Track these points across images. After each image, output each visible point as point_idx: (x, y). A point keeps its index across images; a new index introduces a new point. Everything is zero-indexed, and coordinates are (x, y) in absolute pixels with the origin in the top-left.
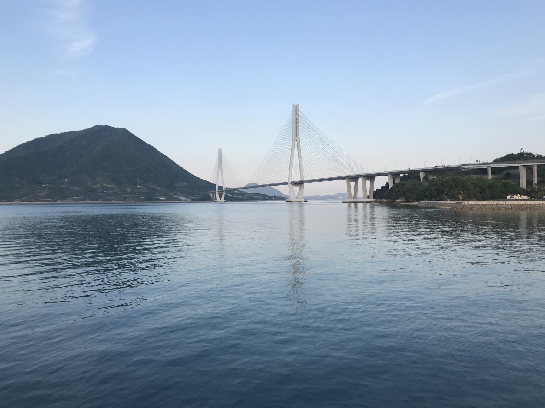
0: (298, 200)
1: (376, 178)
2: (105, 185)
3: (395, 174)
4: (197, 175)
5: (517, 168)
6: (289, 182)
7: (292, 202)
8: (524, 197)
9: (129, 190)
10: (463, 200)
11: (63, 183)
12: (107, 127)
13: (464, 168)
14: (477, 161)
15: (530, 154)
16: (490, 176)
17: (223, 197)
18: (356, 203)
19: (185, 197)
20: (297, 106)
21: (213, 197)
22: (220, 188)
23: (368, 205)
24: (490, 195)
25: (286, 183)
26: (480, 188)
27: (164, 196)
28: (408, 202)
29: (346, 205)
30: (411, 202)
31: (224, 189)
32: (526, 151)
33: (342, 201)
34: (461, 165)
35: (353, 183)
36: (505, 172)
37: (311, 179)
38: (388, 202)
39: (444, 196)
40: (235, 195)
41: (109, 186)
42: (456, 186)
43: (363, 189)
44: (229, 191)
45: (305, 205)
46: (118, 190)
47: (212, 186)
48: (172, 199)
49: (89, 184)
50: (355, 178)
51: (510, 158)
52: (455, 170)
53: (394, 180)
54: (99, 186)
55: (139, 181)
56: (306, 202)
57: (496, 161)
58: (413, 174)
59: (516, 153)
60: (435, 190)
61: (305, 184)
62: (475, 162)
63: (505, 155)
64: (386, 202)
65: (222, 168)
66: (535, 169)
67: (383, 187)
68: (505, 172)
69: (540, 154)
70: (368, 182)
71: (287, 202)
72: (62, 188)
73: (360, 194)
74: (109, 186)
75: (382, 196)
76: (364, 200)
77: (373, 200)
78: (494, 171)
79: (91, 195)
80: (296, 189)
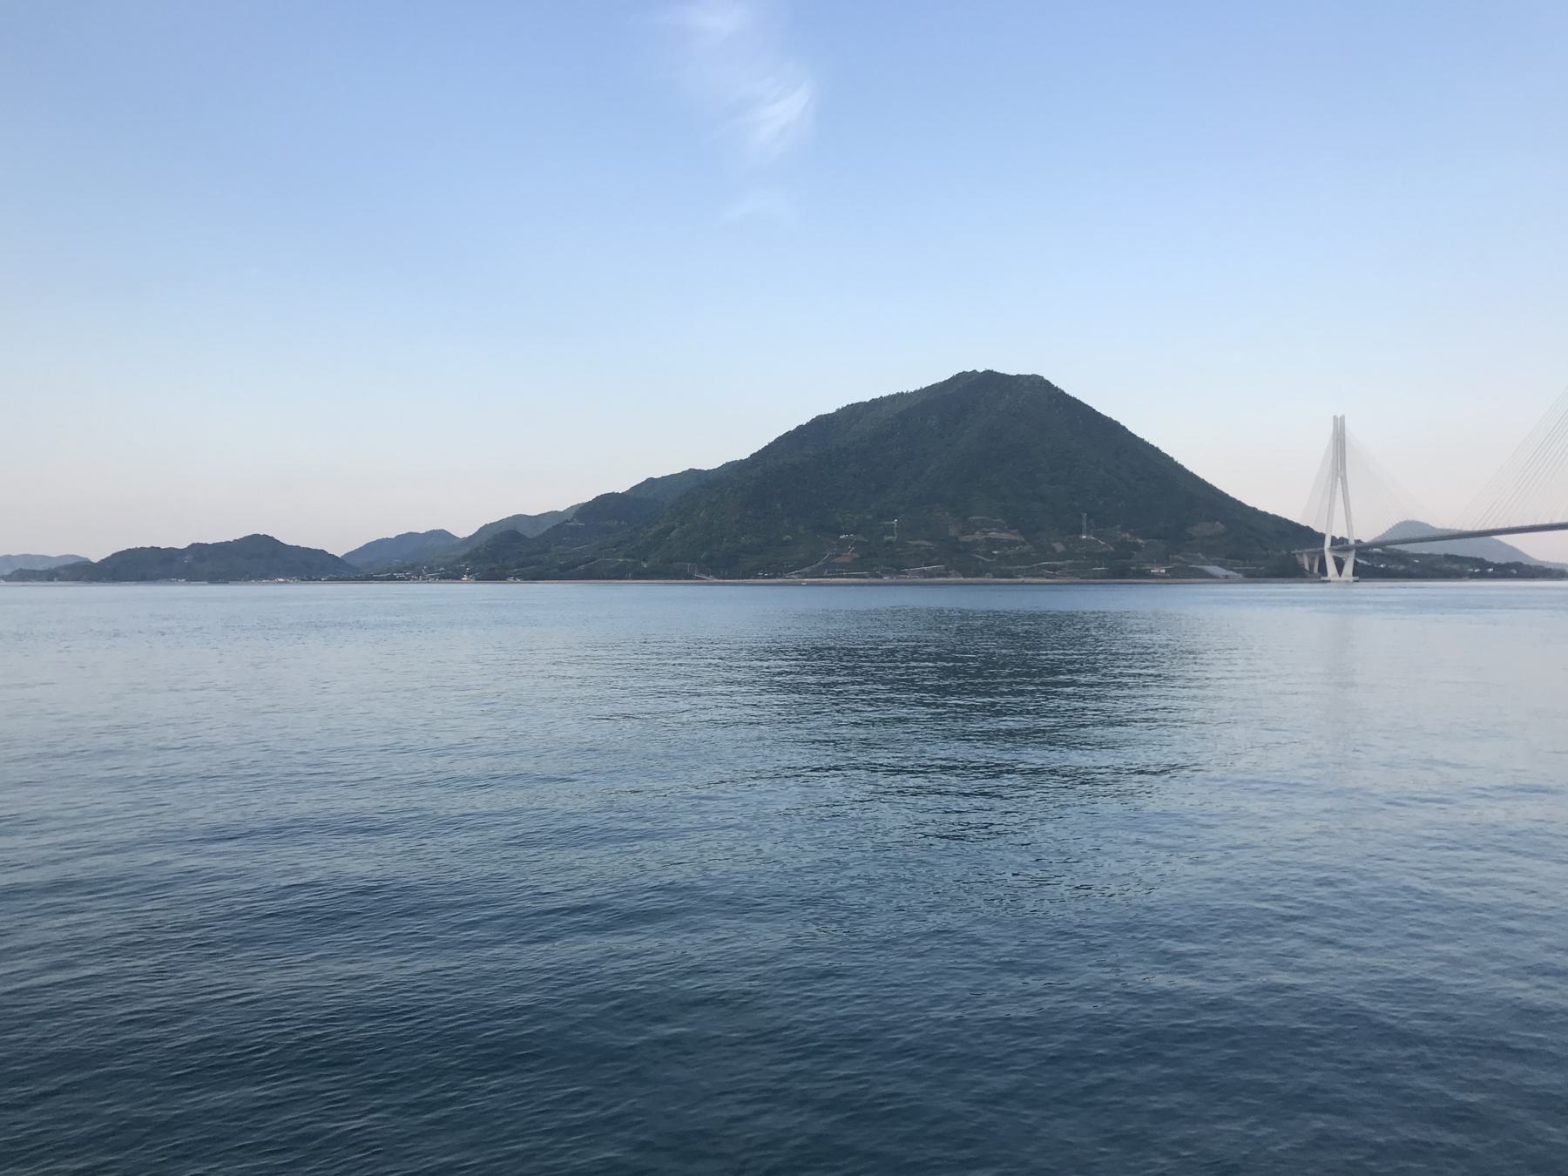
2: (993, 535)
4: (1249, 502)
9: (1060, 547)
11: (889, 530)
12: (990, 375)
17: (1348, 568)
19: (1221, 565)
21: (1311, 566)
27: (1164, 560)
31: (1352, 542)
41: (1005, 536)
44: (1362, 549)
46: (1028, 547)
47: (1309, 537)
48: (1183, 573)
49: (953, 532)
54: (978, 536)
55: (1084, 524)
72: (889, 543)
74: (1005, 536)
79: (964, 563)
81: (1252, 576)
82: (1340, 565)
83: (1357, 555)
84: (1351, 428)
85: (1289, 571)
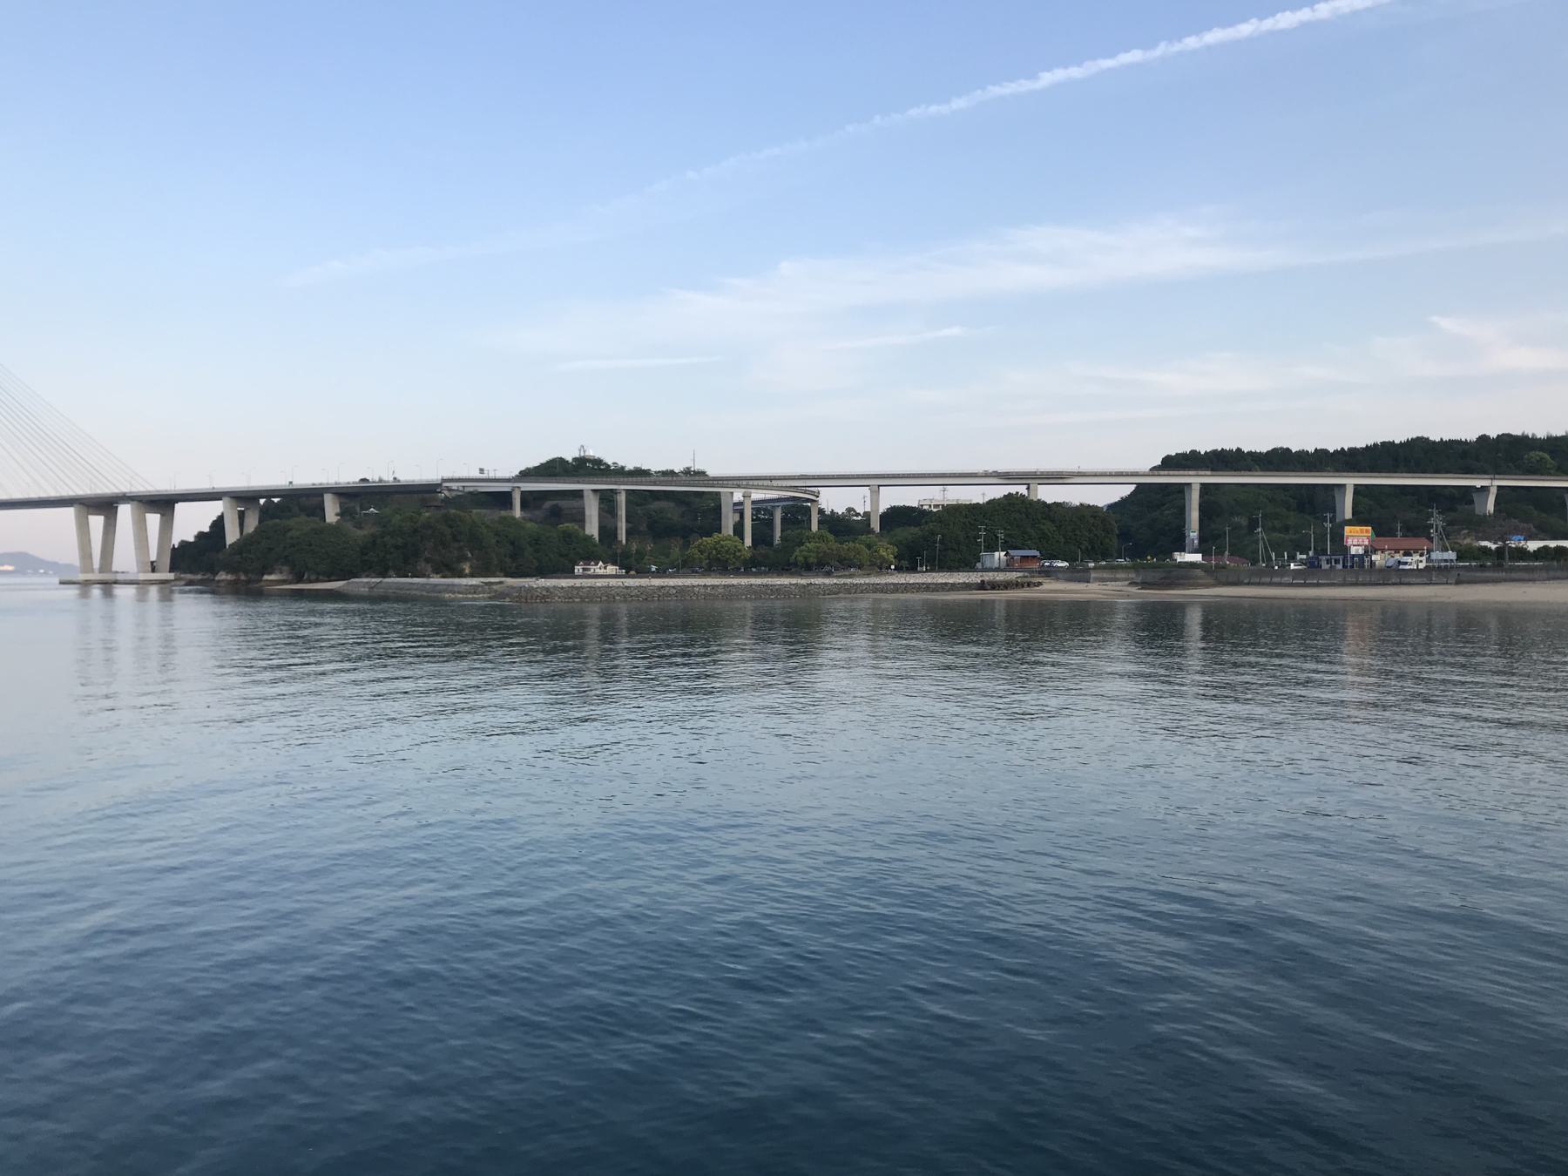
1: (179, 507)
3: (244, 499)
5: (579, 494)
8: (611, 569)
10: (472, 575)
13: (450, 490)
14: (482, 471)
15: (599, 462)
16: (517, 512)
18: (108, 586)
23: (154, 590)
24: (536, 563)
26: (512, 543)
28: (300, 580)
29: (73, 592)
30: (311, 582)
32: (591, 453)
33: (56, 580)
34: (444, 480)
35: (97, 522)
38: (236, 582)
39: (422, 565)
42: (455, 539)
43: (133, 543)
50: (106, 506)
51: (554, 468)
52: (424, 493)
53: (241, 516)
57: (526, 475)
58: (304, 501)
60: (397, 547)
63: (544, 460)
64: (230, 582)
66: (622, 499)
67: (201, 536)
68: (548, 504)
69: (621, 464)
70: (153, 520)
73: (126, 559)
75: (198, 563)
76: (142, 577)
77: (171, 576)
78: (529, 500)
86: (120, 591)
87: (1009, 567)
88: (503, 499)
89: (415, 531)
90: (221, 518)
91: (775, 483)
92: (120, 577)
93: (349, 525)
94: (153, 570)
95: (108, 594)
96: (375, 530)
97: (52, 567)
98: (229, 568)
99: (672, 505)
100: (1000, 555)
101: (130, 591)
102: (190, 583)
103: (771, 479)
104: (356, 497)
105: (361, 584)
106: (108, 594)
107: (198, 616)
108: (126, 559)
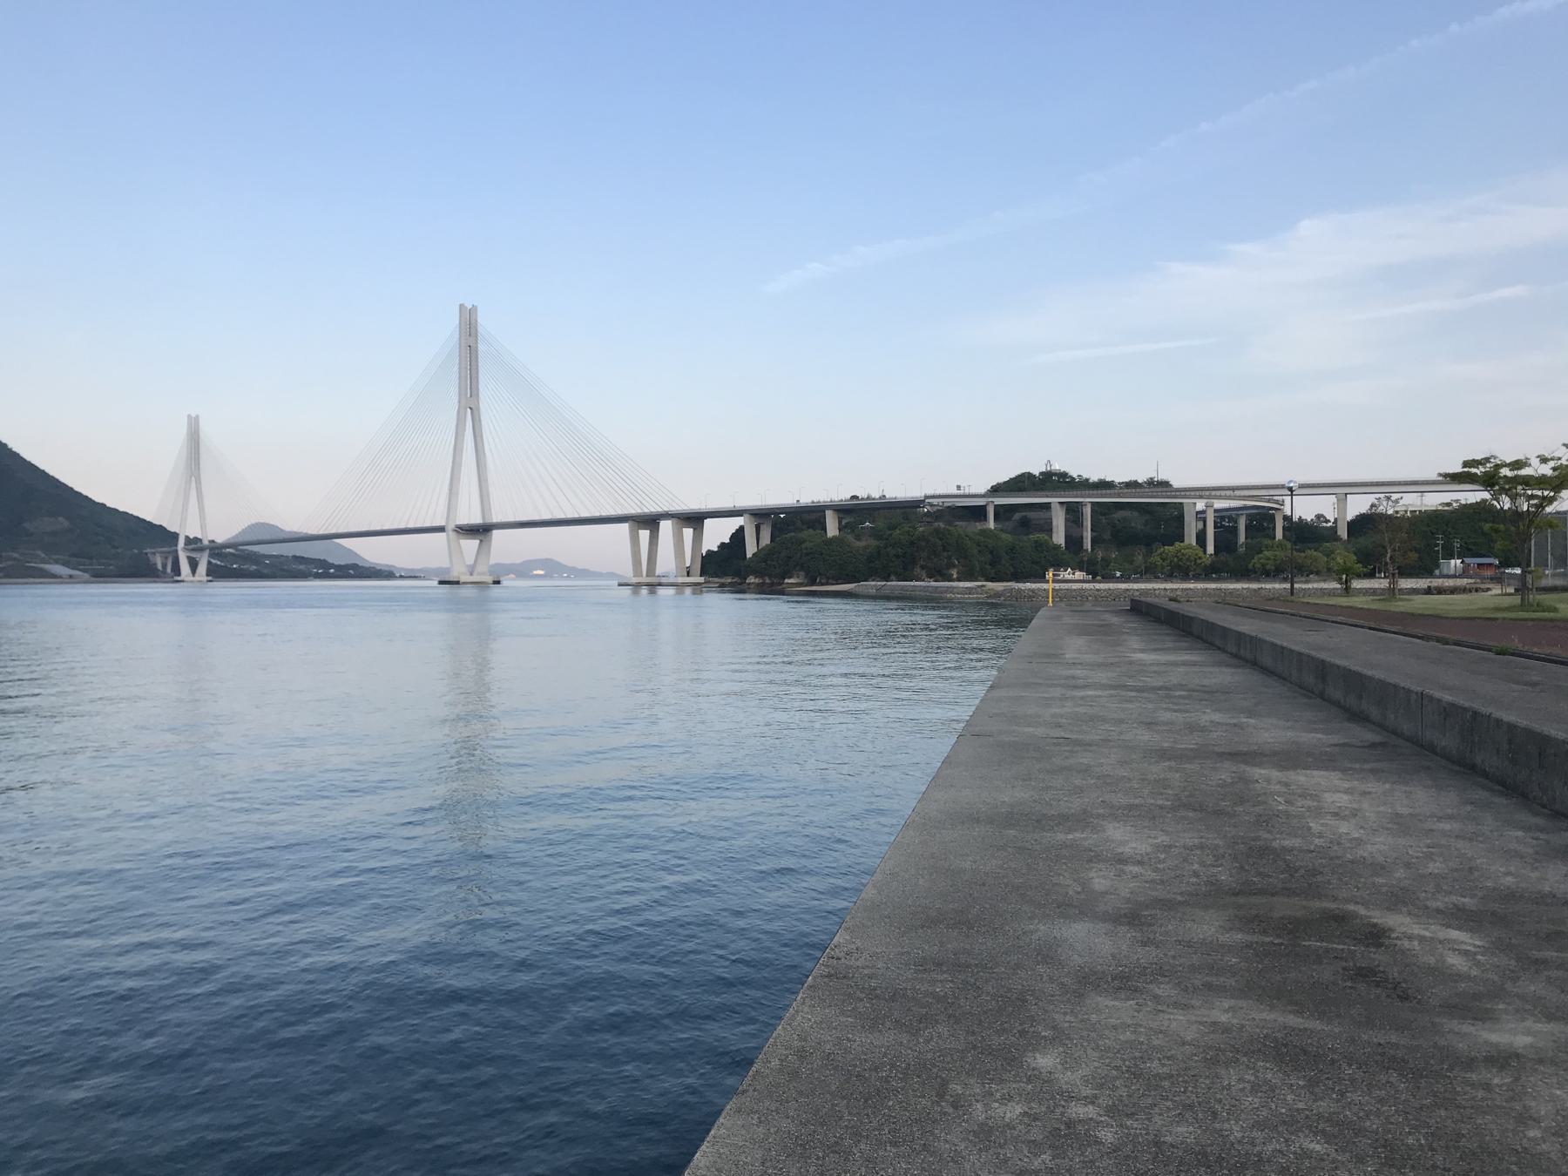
0: (475, 578)
3: (761, 516)
5: (1047, 506)
6: (451, 526)
7: (458, 583)
8: (1079, 575)
10: (959, 580)
13: (931, 505)
14: (959, 487)
15: (1064, 475)
16: (991, 524)
17: (202, 568)
20: (473, 311)
21: (164, 566)
22: (188, 541)
25: (441, 529)
28: (813, 583)
29: (627, 591)
31: (206, 542)
34: (927, 497)
35: (644, 534)
36: (1017, 516)
37: (511, 519)
38: (763, 584)
39: (918, 570)
40: (244, 562)
42: (945, 549)
44: (216, 550)
45: (496, 591)
50: (651, 522)
51: (1023, 483)
52: (907, 509)
56: (498, 582)
57: (996, 490)
58: (807, 517)
59: (1036, 472)
60: (897, 556)
61: (495, 533)
62: (956, 492)
65: (198, 482)
66: (1088, 511)
67: (723, 545)
68: (1017, 516)
69: (1085, 476)
70: (688, 533)
71: (441, 582)
73: (667, 562)
75: (726, 568)
77: (702, 580)
78: (1003, 513)
80: (470, 545)
81: (100, 576)
82: (194, 565)
83: (211, 556)
84: (206, 430)
85: (142, 571)
86: (662, 591)
87: (1464, 574)
88: (978, 513)
89: (912, 543)
90: (741, 529)
91: (1238, 493)
92: (664, 580)
93: (850, 538)
94: (688, 575)
95: (652, 592)
96: (873, 542)
97: (612, 575)
98: (757, 573)
99: (1136, 514)
100: (1456, 563)
101: (671, 591)
102: (722, 585)
103: (1233, 489)
104: (855, 512)
105: (871, 585)
106: (652, 592)
107: (728, 613)
108: (667, 562)
